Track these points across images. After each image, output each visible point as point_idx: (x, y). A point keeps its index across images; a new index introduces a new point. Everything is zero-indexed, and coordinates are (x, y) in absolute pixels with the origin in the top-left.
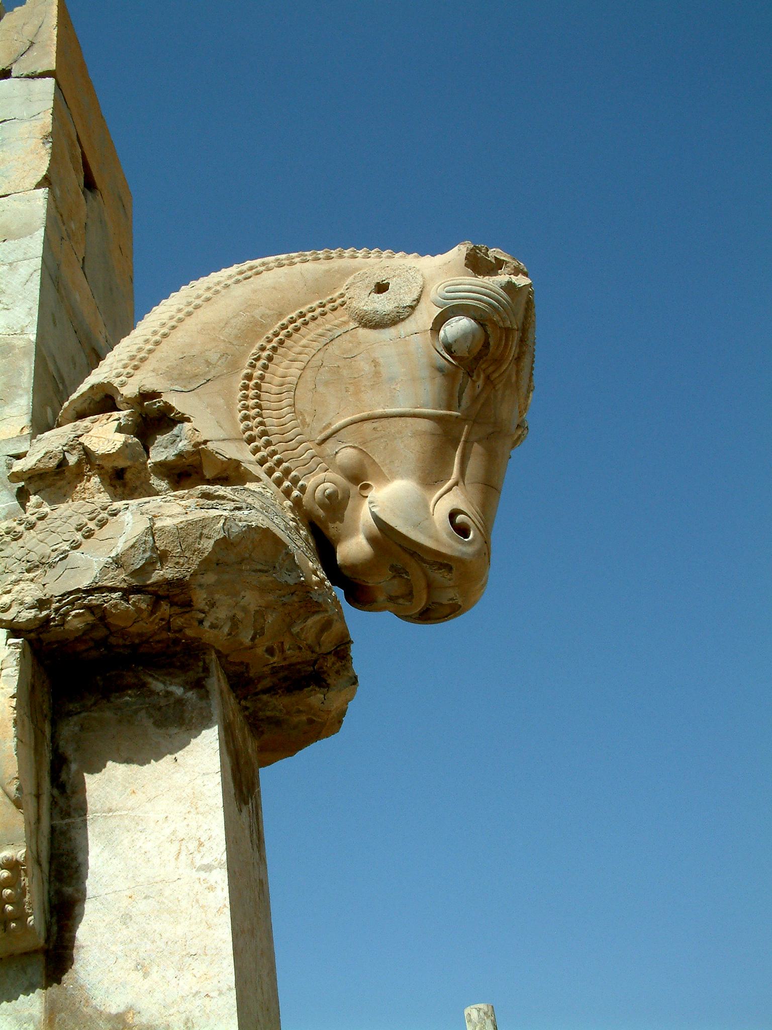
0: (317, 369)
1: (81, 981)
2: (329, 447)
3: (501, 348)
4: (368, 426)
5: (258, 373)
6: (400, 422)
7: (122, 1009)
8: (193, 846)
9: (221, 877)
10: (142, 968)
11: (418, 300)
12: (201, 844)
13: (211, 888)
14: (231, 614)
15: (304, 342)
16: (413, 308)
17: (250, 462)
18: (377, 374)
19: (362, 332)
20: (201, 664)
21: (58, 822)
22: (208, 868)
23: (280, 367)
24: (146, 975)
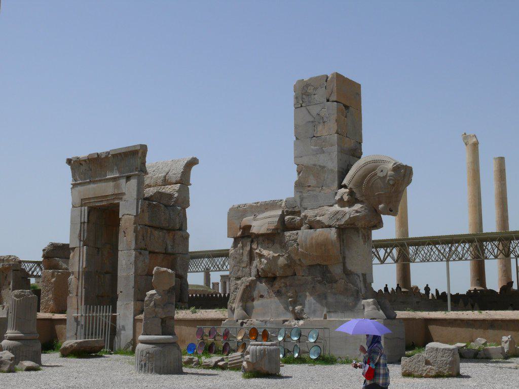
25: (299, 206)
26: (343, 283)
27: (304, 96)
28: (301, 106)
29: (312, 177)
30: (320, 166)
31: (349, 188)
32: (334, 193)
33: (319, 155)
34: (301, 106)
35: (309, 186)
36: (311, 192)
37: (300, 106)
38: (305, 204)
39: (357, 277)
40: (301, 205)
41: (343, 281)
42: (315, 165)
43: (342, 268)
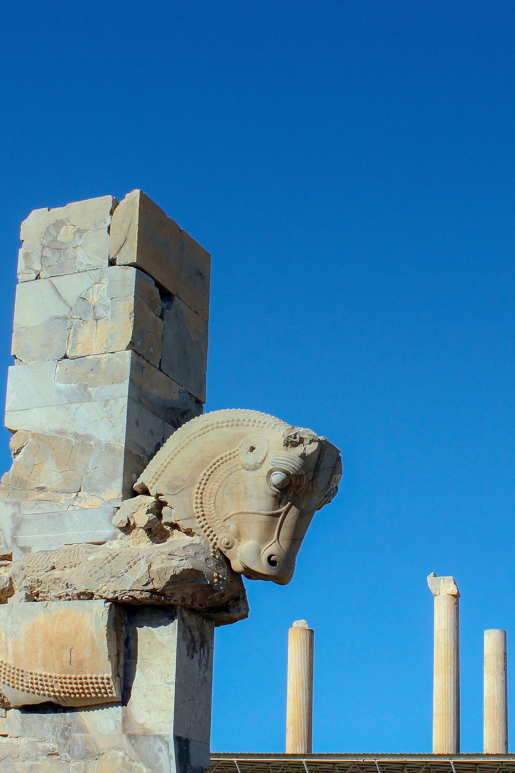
0: (224, 487)
1: (132, 713)
2: (227, 523)
3: (298, 483)
4: (241, 516)
5: (202, 487)
6: (253, 516)
7: (142, 723)
8: (166, 675)
9: (173, 687)
10: (149, 712)
11: (264, 460)
12: (168, 675)
13: (170, 690)
14: (182, 596)
15: (221, 473)
16: (262, 463)
17: (197, 528)
18: (246, 493)
19: (243, 471)
20: (174, 610)
21: (127, 661)
22: (169, 684)
23: (210, 485)
24: (150, 714)
25: (9, 542)
26: (119, 761)
27: (48, 253)
28: (38, 277)
29: (50, 465)
30: (77, 436)
31: (151, 492)
32: (110, 508)
33: (77, 405)
34: (38, 277)
35: (42, 489)
36: (45, 506)
37: (34, 276)
38: (25, 539)
39: (160, 744)
40: (14, 540)
41: (121, 754)
42: (61, 432)
43: (120, 719)
